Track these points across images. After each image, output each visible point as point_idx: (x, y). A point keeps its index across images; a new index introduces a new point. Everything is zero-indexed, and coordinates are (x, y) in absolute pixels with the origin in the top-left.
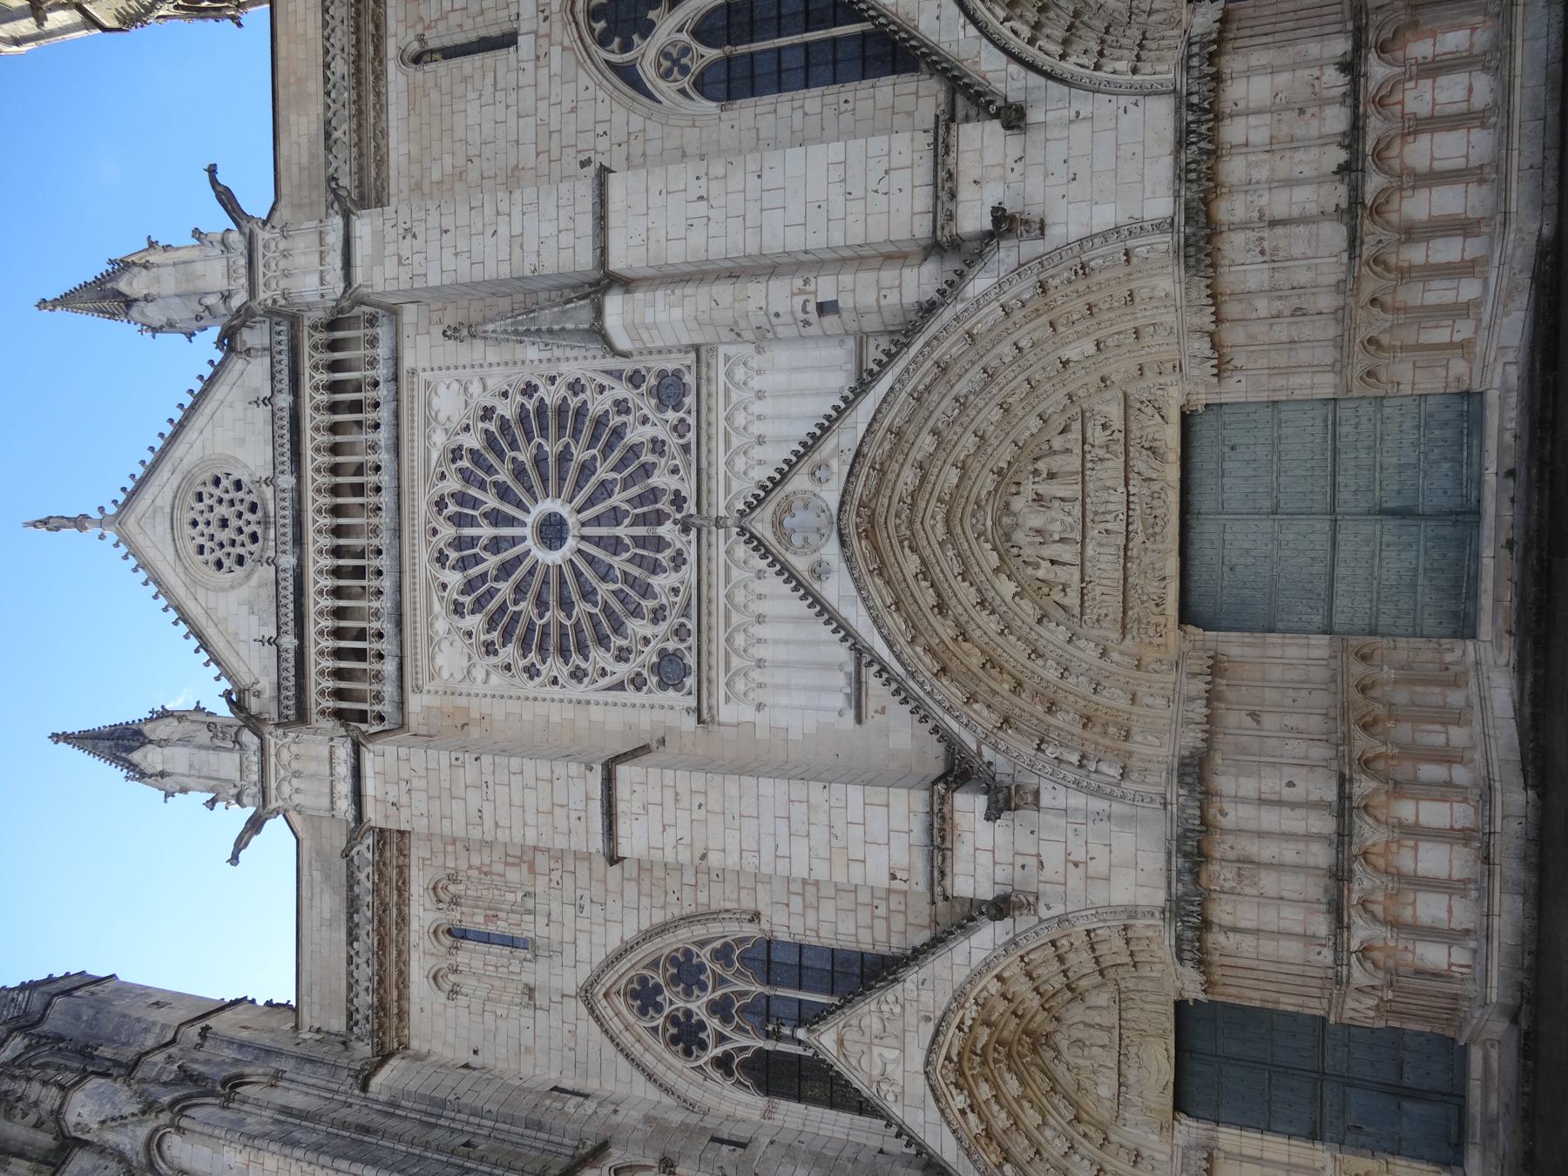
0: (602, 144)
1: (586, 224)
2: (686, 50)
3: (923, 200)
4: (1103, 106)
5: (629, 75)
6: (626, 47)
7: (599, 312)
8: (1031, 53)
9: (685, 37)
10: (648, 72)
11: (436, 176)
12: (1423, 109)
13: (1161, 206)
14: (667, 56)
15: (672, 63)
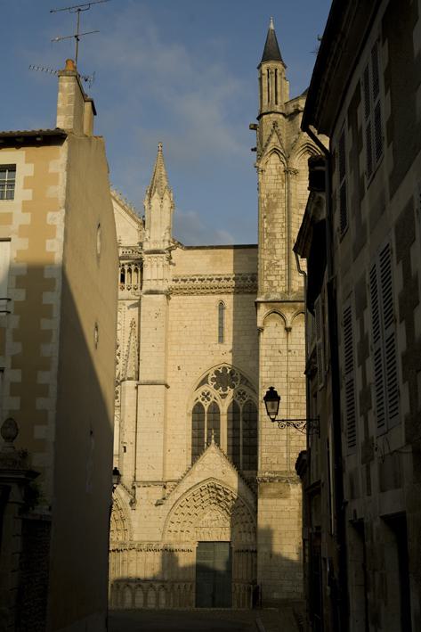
0: (183, 374)
1: (151, 378)
2: (209, 400)
3: (147, 479)
4: (161, 525)
5: (204, 382)
6: (213, 380)
7: (129, 379)
8: (177, 506)
9: (212, 399)
10: (204, 388)
11: (183, 314)
12: (149, 595)
13: (135, 538)
14: (208, 394)
15: (206, 396)
